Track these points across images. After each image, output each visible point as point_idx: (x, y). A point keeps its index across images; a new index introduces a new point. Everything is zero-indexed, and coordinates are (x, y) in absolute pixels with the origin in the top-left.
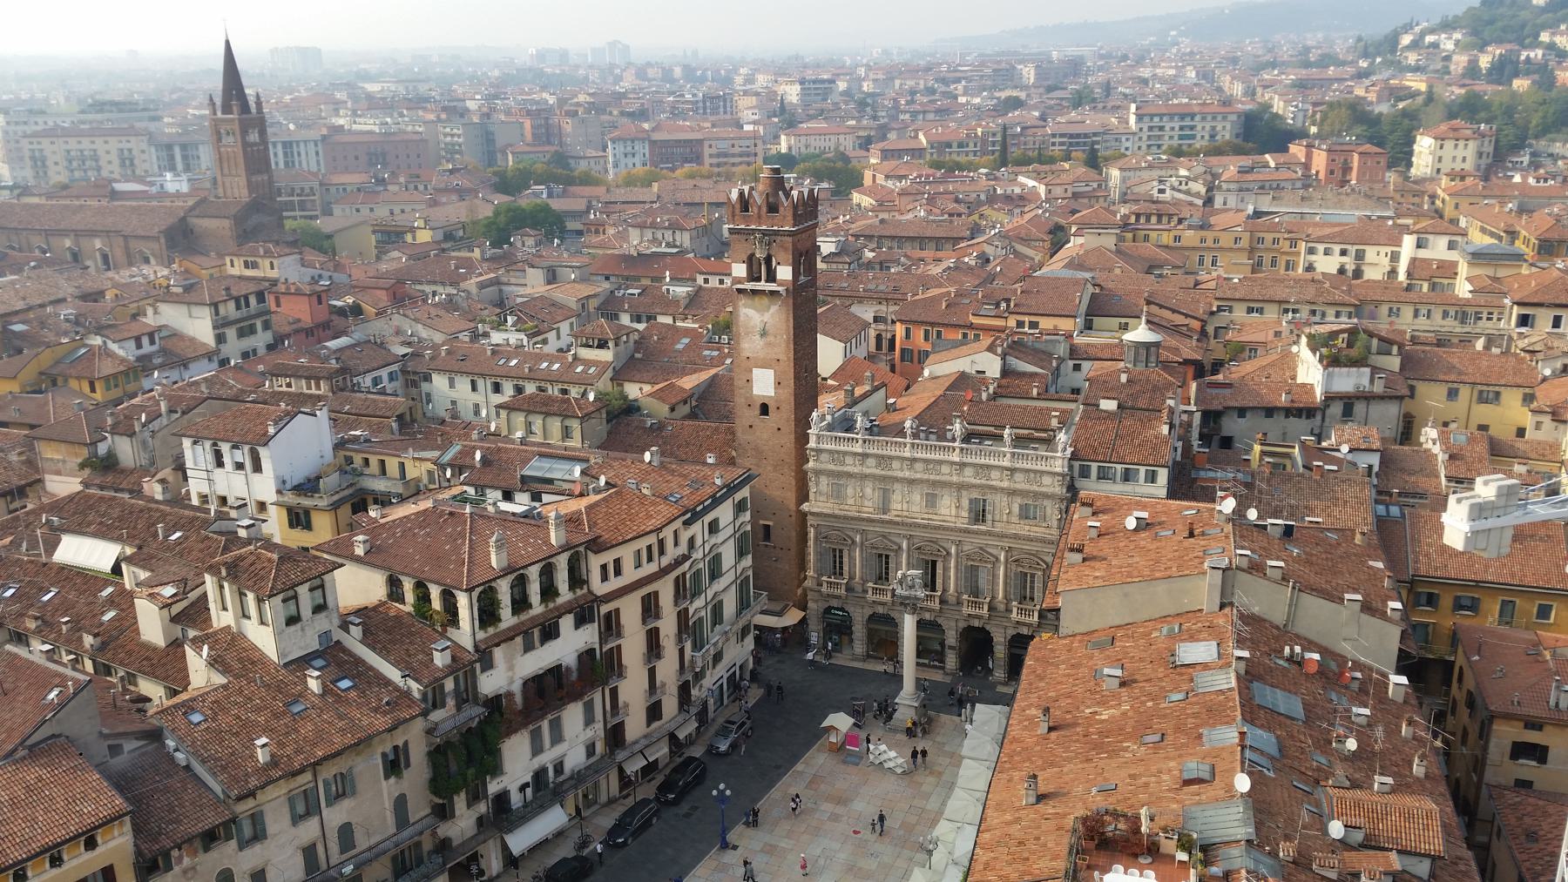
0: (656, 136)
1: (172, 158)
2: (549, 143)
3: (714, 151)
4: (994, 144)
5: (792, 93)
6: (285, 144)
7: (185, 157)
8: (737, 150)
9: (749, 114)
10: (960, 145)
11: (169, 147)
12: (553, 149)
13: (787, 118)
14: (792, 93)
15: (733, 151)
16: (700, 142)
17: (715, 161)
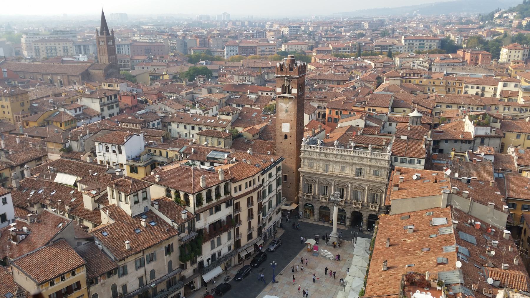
0: (241, 45)
1: (80, 50)
2: (205, 47)
3: (260, 50)
4: (355, 49)
5: (286, 31)
6: (117, 45)
7: (85, 49)
8: (268, 50)
9: (271, 38)
10: (344, 49)
11: (80, 46)
12: (207, 48)
13: (284, 39)
14: (286, 31)
16: (256, 47)
17: (261, 53)
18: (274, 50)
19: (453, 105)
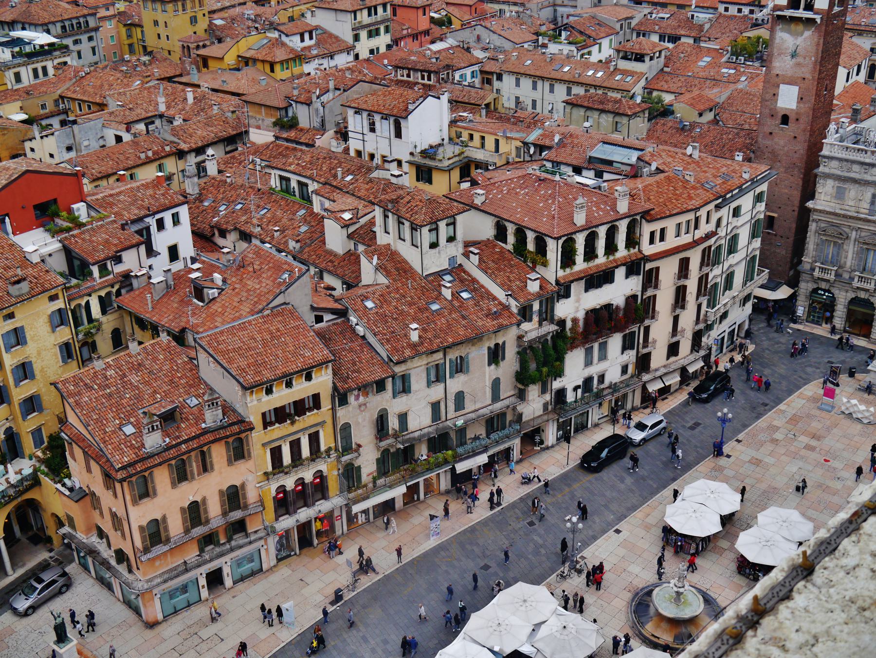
19: (341, 422)
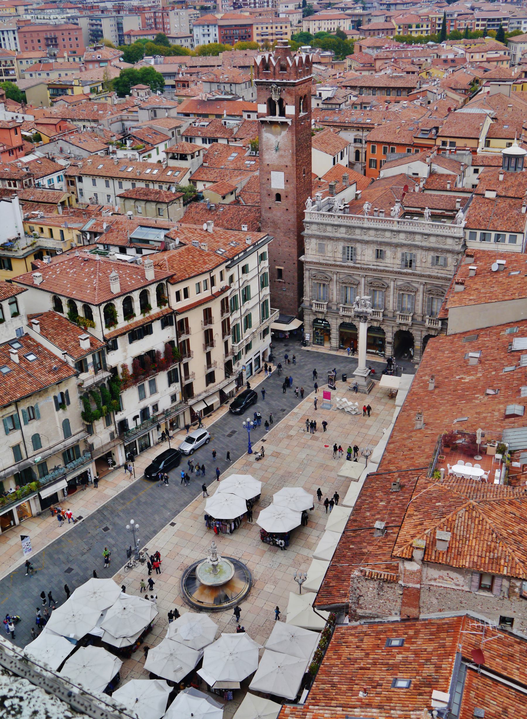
0: (221, 23)
3: (259, 31)
8: (274, 30)
10: (417, 27)
15: (270, 31)
17: (260, 38)
18: (284, 30)
